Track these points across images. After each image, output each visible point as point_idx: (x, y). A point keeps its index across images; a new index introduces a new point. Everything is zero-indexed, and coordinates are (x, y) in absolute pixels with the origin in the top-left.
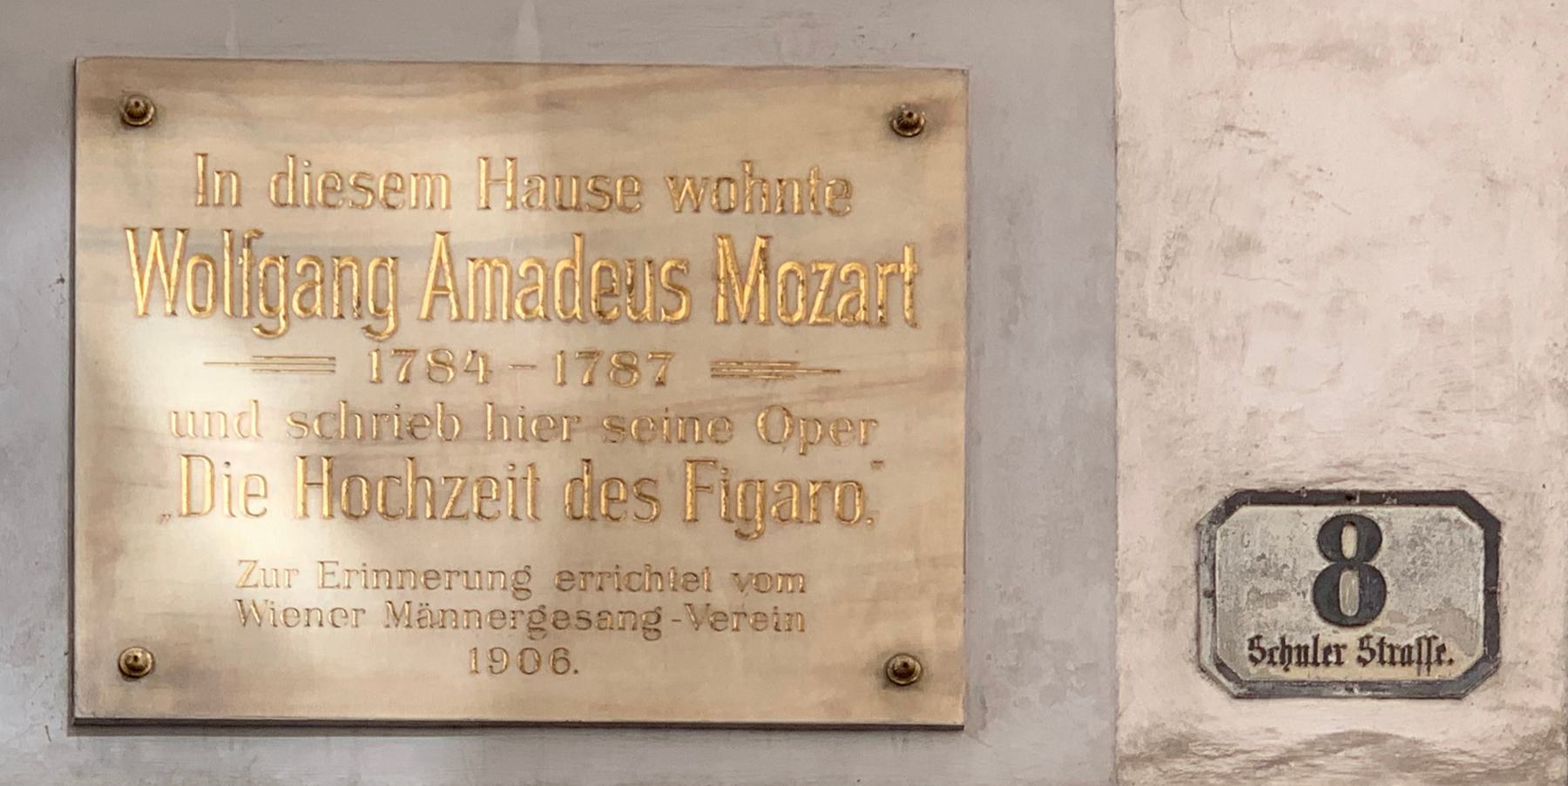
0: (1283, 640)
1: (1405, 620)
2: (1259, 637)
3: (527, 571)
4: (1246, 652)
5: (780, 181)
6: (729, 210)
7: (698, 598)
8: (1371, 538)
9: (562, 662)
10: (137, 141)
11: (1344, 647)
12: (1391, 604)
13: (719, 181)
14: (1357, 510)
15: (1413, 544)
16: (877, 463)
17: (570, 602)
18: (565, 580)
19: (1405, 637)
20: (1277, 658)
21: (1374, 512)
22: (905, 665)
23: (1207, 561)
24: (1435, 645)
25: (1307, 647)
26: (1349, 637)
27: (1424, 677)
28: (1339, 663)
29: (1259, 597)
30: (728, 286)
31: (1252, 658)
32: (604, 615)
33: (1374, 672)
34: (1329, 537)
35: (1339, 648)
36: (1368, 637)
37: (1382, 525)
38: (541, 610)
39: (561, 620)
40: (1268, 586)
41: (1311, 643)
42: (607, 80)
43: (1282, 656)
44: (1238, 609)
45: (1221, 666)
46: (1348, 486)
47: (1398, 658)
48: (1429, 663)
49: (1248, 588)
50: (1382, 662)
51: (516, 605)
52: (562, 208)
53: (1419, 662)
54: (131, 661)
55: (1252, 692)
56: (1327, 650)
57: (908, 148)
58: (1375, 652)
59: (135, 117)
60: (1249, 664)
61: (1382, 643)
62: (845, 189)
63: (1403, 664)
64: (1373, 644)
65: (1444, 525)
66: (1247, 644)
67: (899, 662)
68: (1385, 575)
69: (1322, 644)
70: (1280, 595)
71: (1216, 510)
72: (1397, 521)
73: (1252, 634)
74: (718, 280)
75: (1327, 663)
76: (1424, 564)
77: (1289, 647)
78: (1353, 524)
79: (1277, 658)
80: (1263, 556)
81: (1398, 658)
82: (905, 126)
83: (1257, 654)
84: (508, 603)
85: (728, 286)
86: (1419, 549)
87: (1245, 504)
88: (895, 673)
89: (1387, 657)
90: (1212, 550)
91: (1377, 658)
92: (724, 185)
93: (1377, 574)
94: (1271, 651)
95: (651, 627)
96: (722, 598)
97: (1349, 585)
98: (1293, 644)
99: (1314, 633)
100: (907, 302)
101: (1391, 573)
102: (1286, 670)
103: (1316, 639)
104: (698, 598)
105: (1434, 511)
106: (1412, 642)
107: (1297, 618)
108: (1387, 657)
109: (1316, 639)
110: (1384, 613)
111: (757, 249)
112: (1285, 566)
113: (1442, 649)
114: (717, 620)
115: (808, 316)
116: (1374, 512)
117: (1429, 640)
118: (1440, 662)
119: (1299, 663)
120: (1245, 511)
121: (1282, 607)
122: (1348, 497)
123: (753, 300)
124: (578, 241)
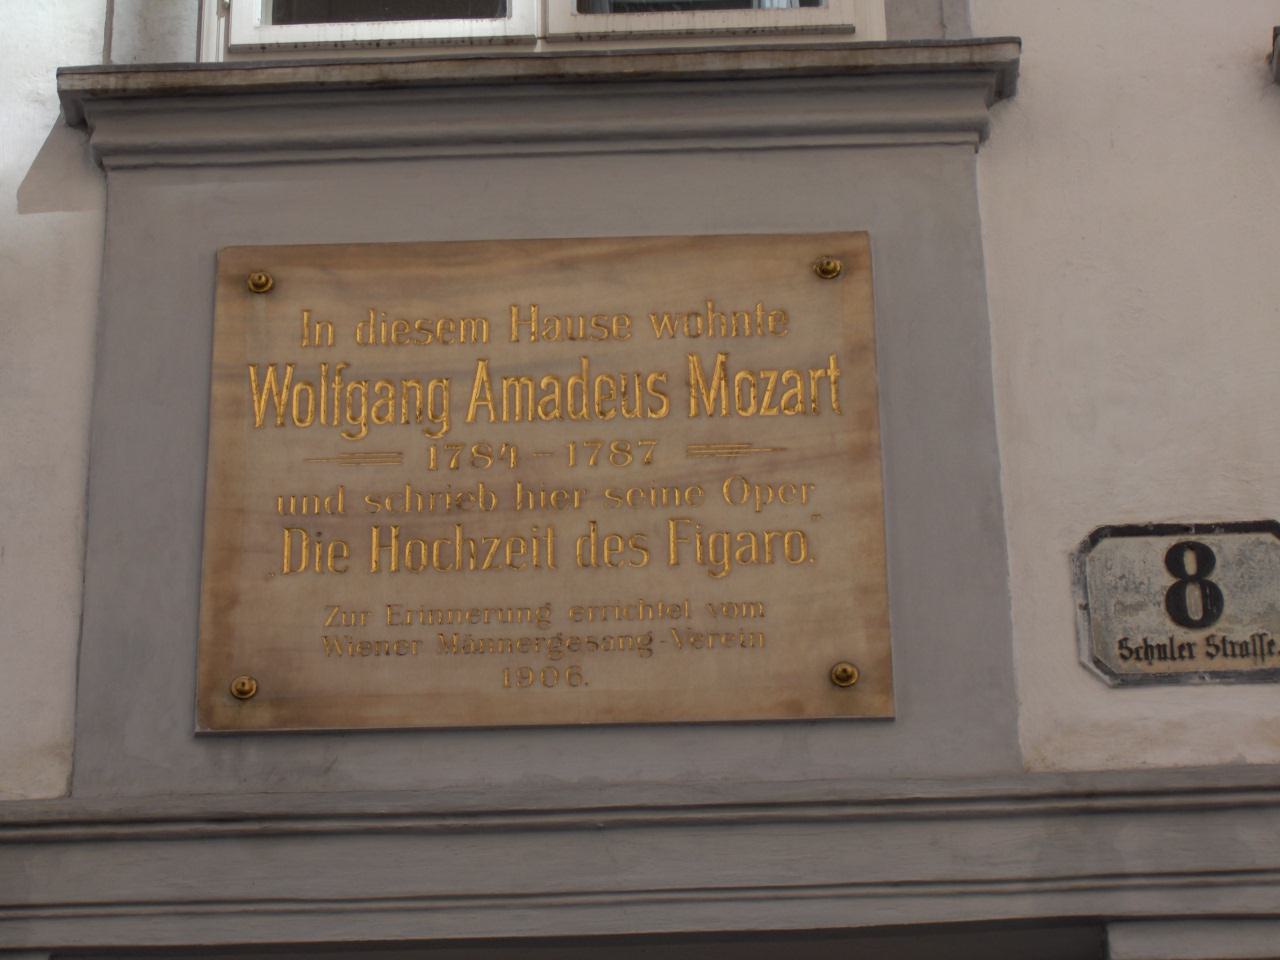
0: (1145, 640)
1: (1240, 621)
2: (1126, 639)
3: (548, 606)
4: (1116, 651)
5: (735, 314)
6: (698, 336)
7: (681, 623)
8: (1206, 558)
9: (575, 676)
10: (260, 303)
11: (1194, 644)
12: (1229, 608)
13: (689, 316)
14: (1193, 538)
15: (1240, 563)
16: (816, 516)
17: (583, 630)
18: (578, 614)
19: (1241, 634)
20: (1142, 655)
21: (1207, 540)
22: (845, 671)
23: (1081, 581)
24: (1266, 640)
25: (1164, 646)
26: (1196, 636)
27: (1260, 666)
28: (1191, 656)
29: (1124, 608)
30: (698, 390)
31: (1123, 656)
32: (608, 639)
33: (1220, 663)
34: (1173, 560)
35: (1190, 645)
36: (1213, 636)
37: (1214, 549)
38: (559, 638)
39: (575, 645)
40: (1130, 599)
41: (1167, 642)
42: (604, 249)
43: (1146, 653)
44: (1107, 617)
45: (1097, 662)
46: (1185, 522)
47: (1237, 651)
48: (1262, 654)
49: (1113, 601)
50: (1225, 655)
51: (541, 634)
52: (572, 339)
53: (1255, 654)
54: (239, 686)
55: (1124, 682)
56: (1181, 647)
57: (829, 287)
58: (1222, 648)
59: (259, 289)
60: (1120, 661)
61: (1224, 640)
62: (783, 317)
63: (1243, 656)
64: (1218, 641)
65: (1263, 547)
66: (1117, 645)
67: (840, 669)
68: (1221, 587)
69: (1177, 644)
70: (1139, 607)
71: (1084, 542)
72: (1224, 546)
73: (1120, 637)
74: (688, 384)
75: (1182, 657)
76: (1251, 578)
77: (1151, 646)
78: (1192, 549)
79: (1142, 655)
80: (1123, 577)
81: (1237, 651)
82: (824, 273)
83: (1126, 653)
84: (532, 632)
85: (698, 390)
86: (1245, 566)
87: (1106, 536)
88: (838, 678)
89: (1229, 651)
90: (1083, 572)
91: (1221, 653)
92: (692, 318)
93: (1214, 587)
94: (1137, 650)
95: (647, 646)
96: (699, 623)
97: (1193, 597)
98: (1154, 644)
99: (1170, 635)
100: (833, 396)
101: (1226, 586)
102: (1150, 664)
103: (1171, 640)
104: (681, 623)
105: (1252, 537)
106: (1248, 639)
107: (1154, 624)
108: (1229, 651)
109: (1171, 640)
110: (1223, 617)
111: (719, 362)
112: (1141, 583)
113: (1271, 643)
114: (696, 640)
115: (759, 410)
116: (1207, 540)
117: (1261, 637)
118: (1271, 653)
119: (1160, 658)
120: (1106, 543)
121: (1142, 614)
122: (1184, 529)
123: (718, 399)
124: (585, 361)
